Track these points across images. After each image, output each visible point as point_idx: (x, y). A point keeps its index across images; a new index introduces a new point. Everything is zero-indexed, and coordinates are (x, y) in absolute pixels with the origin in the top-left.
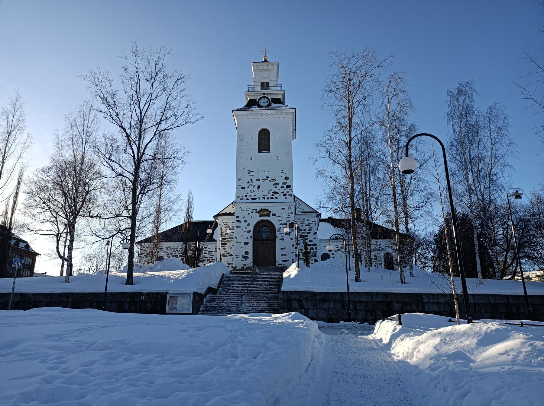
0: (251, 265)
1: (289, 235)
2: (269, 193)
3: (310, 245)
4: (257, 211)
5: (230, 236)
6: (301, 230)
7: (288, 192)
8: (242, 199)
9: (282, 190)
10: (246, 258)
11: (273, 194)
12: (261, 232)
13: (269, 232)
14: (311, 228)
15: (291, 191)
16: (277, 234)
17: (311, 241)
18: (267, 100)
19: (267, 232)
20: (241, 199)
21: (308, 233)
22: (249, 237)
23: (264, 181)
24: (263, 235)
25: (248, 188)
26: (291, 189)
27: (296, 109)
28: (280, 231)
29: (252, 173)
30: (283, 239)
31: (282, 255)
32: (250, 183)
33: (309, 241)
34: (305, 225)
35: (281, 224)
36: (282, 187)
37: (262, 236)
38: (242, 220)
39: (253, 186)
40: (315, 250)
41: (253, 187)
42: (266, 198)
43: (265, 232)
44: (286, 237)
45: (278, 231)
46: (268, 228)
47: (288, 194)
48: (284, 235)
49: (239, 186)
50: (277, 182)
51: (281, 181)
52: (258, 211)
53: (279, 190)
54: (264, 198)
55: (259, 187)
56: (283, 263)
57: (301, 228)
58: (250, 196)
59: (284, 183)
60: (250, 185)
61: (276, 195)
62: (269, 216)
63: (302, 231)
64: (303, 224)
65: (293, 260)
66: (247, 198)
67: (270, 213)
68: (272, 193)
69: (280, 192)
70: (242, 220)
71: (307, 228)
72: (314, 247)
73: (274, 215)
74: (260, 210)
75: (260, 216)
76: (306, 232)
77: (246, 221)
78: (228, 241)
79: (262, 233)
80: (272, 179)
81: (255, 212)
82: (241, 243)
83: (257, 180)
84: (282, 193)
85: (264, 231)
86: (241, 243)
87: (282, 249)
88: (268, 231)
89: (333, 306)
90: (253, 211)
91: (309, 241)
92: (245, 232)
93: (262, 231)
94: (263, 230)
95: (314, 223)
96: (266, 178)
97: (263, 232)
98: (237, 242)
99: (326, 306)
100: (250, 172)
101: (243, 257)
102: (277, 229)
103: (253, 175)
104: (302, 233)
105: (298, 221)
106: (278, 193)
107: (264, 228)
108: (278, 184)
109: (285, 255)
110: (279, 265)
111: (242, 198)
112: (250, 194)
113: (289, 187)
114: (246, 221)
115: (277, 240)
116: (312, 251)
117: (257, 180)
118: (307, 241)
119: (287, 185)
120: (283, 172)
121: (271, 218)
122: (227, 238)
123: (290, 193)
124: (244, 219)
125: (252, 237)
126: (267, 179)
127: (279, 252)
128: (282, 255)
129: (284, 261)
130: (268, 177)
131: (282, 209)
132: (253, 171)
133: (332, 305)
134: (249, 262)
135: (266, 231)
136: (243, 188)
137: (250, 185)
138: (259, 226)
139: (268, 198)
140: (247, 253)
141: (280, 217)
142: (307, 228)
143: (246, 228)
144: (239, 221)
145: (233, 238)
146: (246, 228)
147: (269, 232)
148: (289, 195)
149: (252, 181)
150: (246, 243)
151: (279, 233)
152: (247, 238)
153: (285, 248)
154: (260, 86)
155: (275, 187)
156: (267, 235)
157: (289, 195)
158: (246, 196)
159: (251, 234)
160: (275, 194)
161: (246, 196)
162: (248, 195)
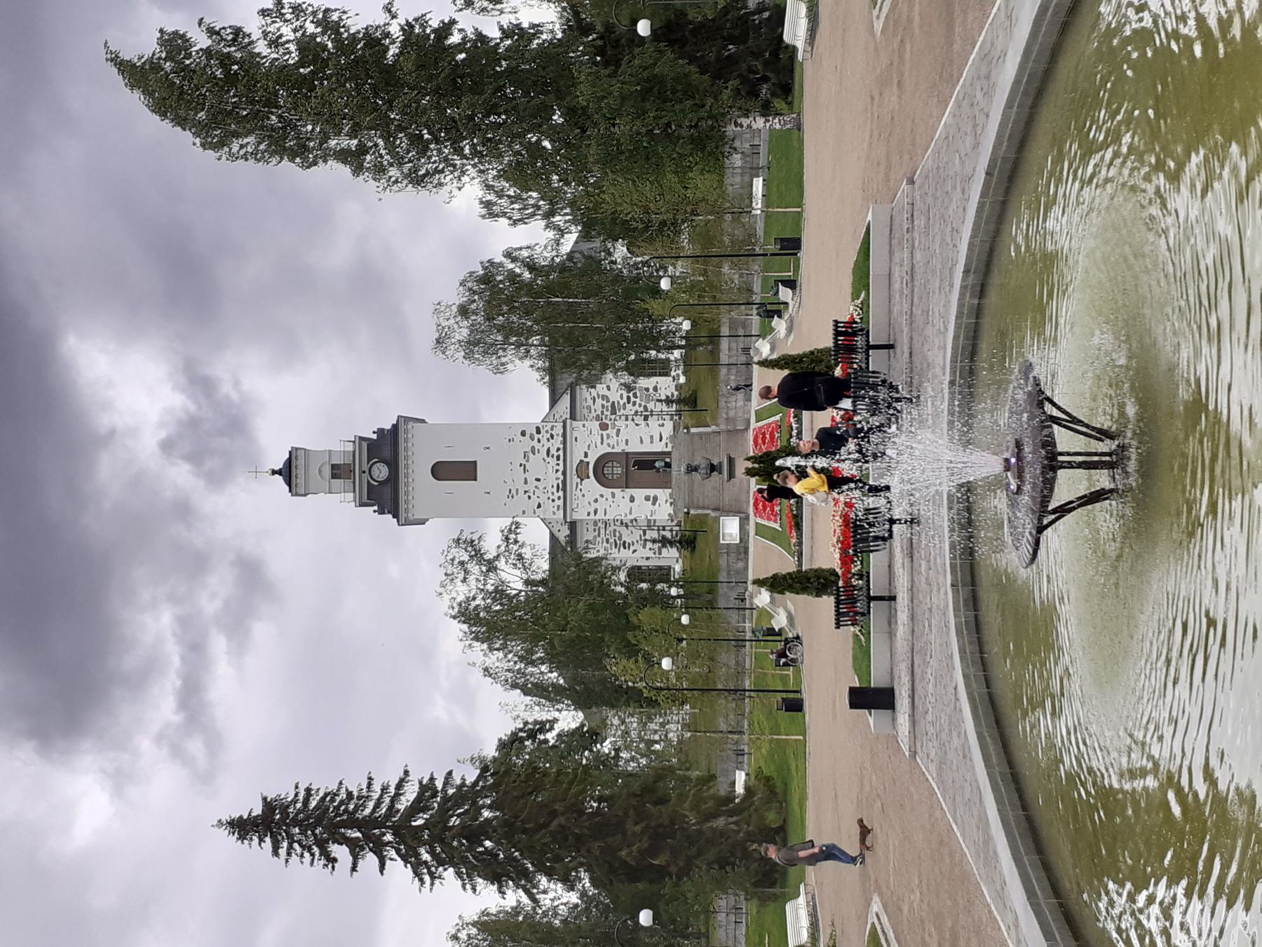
3: (628, 398)
6: (602, 413)
7: (547, 432)
8: (558, 507)
9: (544, 441)
10: (655, 499)
14: (598, 395)
17: (622, 395)
19: (613, 467)
29: (514, 492)
30: (627, 441)
31: (652, 442)
32: (531, 495)
35: (602, 443)
36: (539, 441)
38: (594, 506)
44: (623, 437)
45: (613, 448)
48: (620, 438)
51: (527, 443)
52: (579, 480)
54: (557, 471)
55: (538, 480)
56: (664, 440)
57: (599, 413)
58: (553, 493)
59: (532, 438)
61: (553, 451)
62: (588, 463)
64: (593, 408)
69: (549, 444)
70: (594, 506)
71: (599, 402)
73: (586, 455)
75: (588, 477)
77: (596, 501)
78: (620, 538)
83: (526, 482)
84: (548, 440)
87: (642, 441)
97: (613, 474)
100: (511, 495)
101: (654, 504)
102: (610, 450)
103: (517, 490)
108: (533, 447)
109: (652, 437)
113: (538, 431)
114: (596, 501)
115: (629, 449)
116: (638, 394)
117: (526, 482)
121: (592, 460)
123: (549, 428)
124: (592, 503)
127: (647, 448)
128: (652, 442)
129: (661, 440)
134: (663, 494)
136: (539, 506)
138: (602, 480)
140: (647, 498)
142: (599, 402)
144: (596, 512)
145: (615, 530)
148: (552, 430)
150: (632, 499)
157: (552, 430)
161: (553, 501)
162: (552, 497)
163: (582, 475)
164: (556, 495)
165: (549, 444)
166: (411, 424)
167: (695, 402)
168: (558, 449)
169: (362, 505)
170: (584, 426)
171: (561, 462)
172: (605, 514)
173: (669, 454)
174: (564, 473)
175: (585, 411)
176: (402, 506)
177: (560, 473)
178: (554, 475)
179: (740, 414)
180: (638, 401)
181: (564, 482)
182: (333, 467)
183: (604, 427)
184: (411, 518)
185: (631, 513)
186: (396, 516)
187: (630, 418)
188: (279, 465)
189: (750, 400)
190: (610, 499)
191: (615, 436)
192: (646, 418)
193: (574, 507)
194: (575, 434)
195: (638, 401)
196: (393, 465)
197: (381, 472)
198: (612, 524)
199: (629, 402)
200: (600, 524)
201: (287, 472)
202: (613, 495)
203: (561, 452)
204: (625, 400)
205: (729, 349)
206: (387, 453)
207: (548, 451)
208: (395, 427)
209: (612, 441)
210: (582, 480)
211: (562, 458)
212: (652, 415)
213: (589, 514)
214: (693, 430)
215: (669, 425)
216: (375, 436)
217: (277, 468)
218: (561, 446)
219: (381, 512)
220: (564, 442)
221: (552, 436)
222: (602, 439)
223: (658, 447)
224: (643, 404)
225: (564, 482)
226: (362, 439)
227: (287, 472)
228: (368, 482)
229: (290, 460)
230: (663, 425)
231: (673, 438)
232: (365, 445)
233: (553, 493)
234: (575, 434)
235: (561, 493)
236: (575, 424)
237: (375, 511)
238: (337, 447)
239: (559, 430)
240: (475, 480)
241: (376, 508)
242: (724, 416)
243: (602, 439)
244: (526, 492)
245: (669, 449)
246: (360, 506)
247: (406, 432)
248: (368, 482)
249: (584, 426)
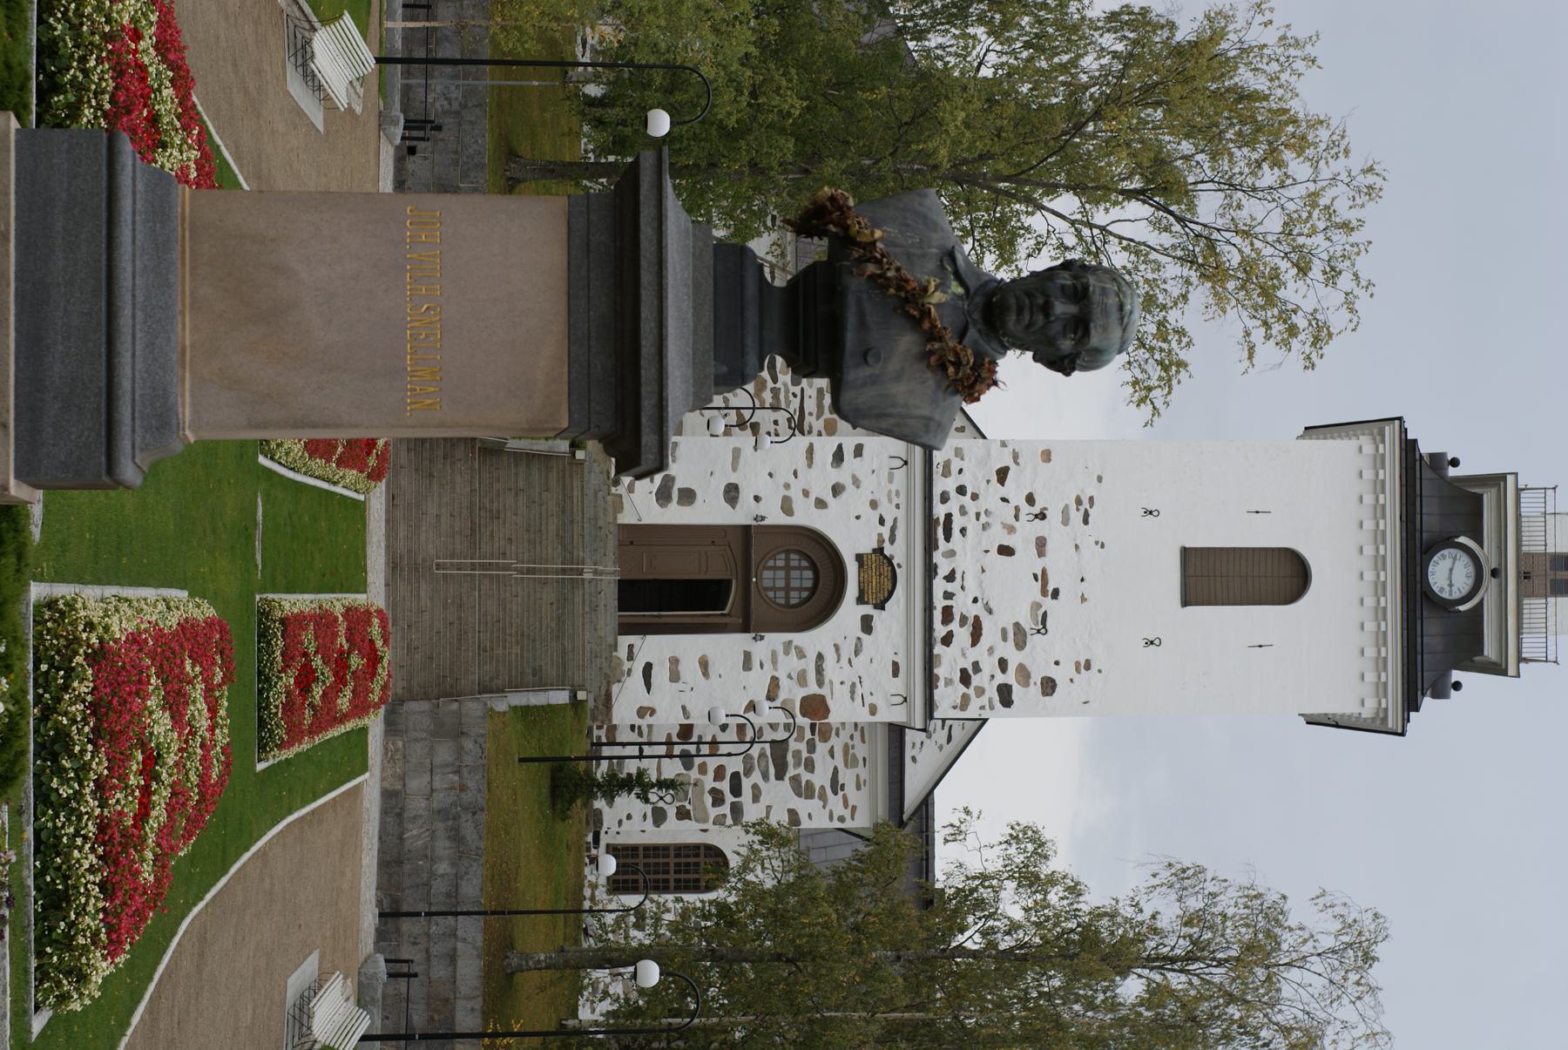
0: (626, 518)
1: (771, 697)
2: (975, 600)
3: (736, 790)
4: (887, 545)
5: (787, 391)
6: (811, 747)
7: (980, 692)
8: (946, 473)
9: (989, 665)
11: (971, 621)
12: (787, 560)
13: (787, 598)
14: (823, 797)
15: (982, 708)
16: (775, 640)
18: (1465, 590)
19: (787, 589)
20: (947, 465)
21: (795, 780)
22: (761, 509)
23: (1035, 577)
24: (775, 568)
25: (1004, 500)
26: (992, 708)
27: (1402, 734)
28: (787, 652)
29: (1078, 518)
31: (674, 662)
32: (1025, 508)
33: (755, 787)
34: (836, 769)
35: (820, 657)
36: (1003, 664)
37: (771, 563)
38: (843, 475)
39: (1011, 521)
40: (713, 812)
41: (1005, 526)
42: (950, 587)
43: (788, 578)
45: (788, 645)
46: (805, 594)
47: (971, 691)
48: (769, 672)
49: (1015, 457)
50: (1034, 641)
51: (1039, 656)
53: (991, 650)
54: (950, 577)
55: (1005, 551)
57: (822, 748)
58: (963, 511)
59: (1024, 674)
60: (1017, 509)
61: (962, 635)
62: (861, 600)
63: (805, 755)
64: (839, 760)
65: (653, 712)
66: (953, 494)
67: (876, 607)
68: (977, 618)
69: (975, 654)
70: (843, 475)
71: (821, 778)
72: (725, 809)
73: (867, 624)
74: (889, 560)
75: (859, 558)
76: (801, 770)
77: (837, 490)
79: (780, 563)
80: (1045, 614)
81: (880, 535)
82: (734, 469)
83: (1041, 545)
84: (976, 667)
85: (795, 574)
86: (734, 469)
87: (704, 665)
88: (794, 594)
89: (441, 871)
90: (889, 523)
91: (755, 787)
92: (787, 486)
93: (794, 563)
94: (800, 568)
95: (847, 813)
96: (1050, 588)
97: (788, 568)
98: (736, 453)
99: (443, 846)
100: (1085, 509)
102: (798, 638)
103: (1066, 521)
104: (797, 753)
105: (857, 735)
106: (974, 644)
107: (809, 574)
108: (1020, 644)
109: (675, 677)
110: (631, 647)
111: (954, 469)
112: (972, 507)
114: (837, 490)
116: (708, 800)
117: (1041, 545)
118: (756, 777)
119: (1016, 689)
120: (1078, 670)
121: (849, 611)
122: (775, 380)
123: (975, 703)
124: (847, 481)
125: (762, 523)
126: (1044, 592)
127: (689, 646)
128: (674, 662)
129: (648, 670)
130: (1056, 594)
131: (896, 666)
132: (1086, 521)
133: (443, 868)
135: (795, 584)
136: (1002, 474)
137: (1017, 509)
139: (948, 595)
140: (688, 496)
141: (857, 653)
142: (821, 778)
143: (806, 493)
144: (838, 457)
146: (806, 493)
147: (787, 598)
149: (1036, 516)
151: (780, 649)
152: (757, 499)
153: (706, 673)
154: (1550, 550)
155: (1004, 631)
156: (774, 589)
158: (961, 490)
159: (776, 517)
160: (968, 629)
162: (967, 500)
163: (879, 567)
164: (953, 507)
165: (975, 654)
166: (1368, 711)
167: (555, 789)
168: (947, 640)
169: (1498, 480)
170: (873, 710)
171: (939, 603)
172: (810, 451)
173: (626, 629)
174: (930, 570)
175: (861, 751)
176: (1391, 474)
177: (943, 571)
178: (960, 564)
179: (418, 750)
180: (709, 782)
181: (930, 546)
183: (815, 707)
184: (1366, 442)
185: (736, 453)
186: (1409, 447)
187: (732, 735)
189: (388, 795)
190: (795, 494)
191: (784, 682)
192: (686, 731)
193: (900, 475)
194: (898, 685)
195: (709, 782)
198: (783, 424)
199: (736, 777)
200: (818, 425)
202: (787, 506)
203: (940, 630)
204: (746, 784)
205: (452, 958)
206: (1433, 631)
207: (976, 636)
209: (789, 664)
210: (879, 551)
211: (938, 615)
212: (669, 743)
213: (858, 451)
214: (561, 697)
215: (623, 712)
216: (1456, 675)
218: (938, 649)
219: (1438, 461)
220: (930, 661)
221: (965, 679)
222: (819, 671)
223: (655, 648)
224: (694, 774)
225: (930, 546)
226: (1498, 669)
228: (1480, 543)
230: (642, 712)
231: (611, 675)
232: (1490, 651)
233: (963, 511)
234: (898, 685)
235: (940, 511)
236: (898, 716)
237: (1455, 463)
239: (946, 698)
240: (1185, 552)
241: (1452, 472)
242: (468, 744)
243: (819, 671)
244: (1042, 516)
245: (625, 641)
246: (1502, 478)
247: (1381, 689)
248: (1480, 543)
249: (873, 710)
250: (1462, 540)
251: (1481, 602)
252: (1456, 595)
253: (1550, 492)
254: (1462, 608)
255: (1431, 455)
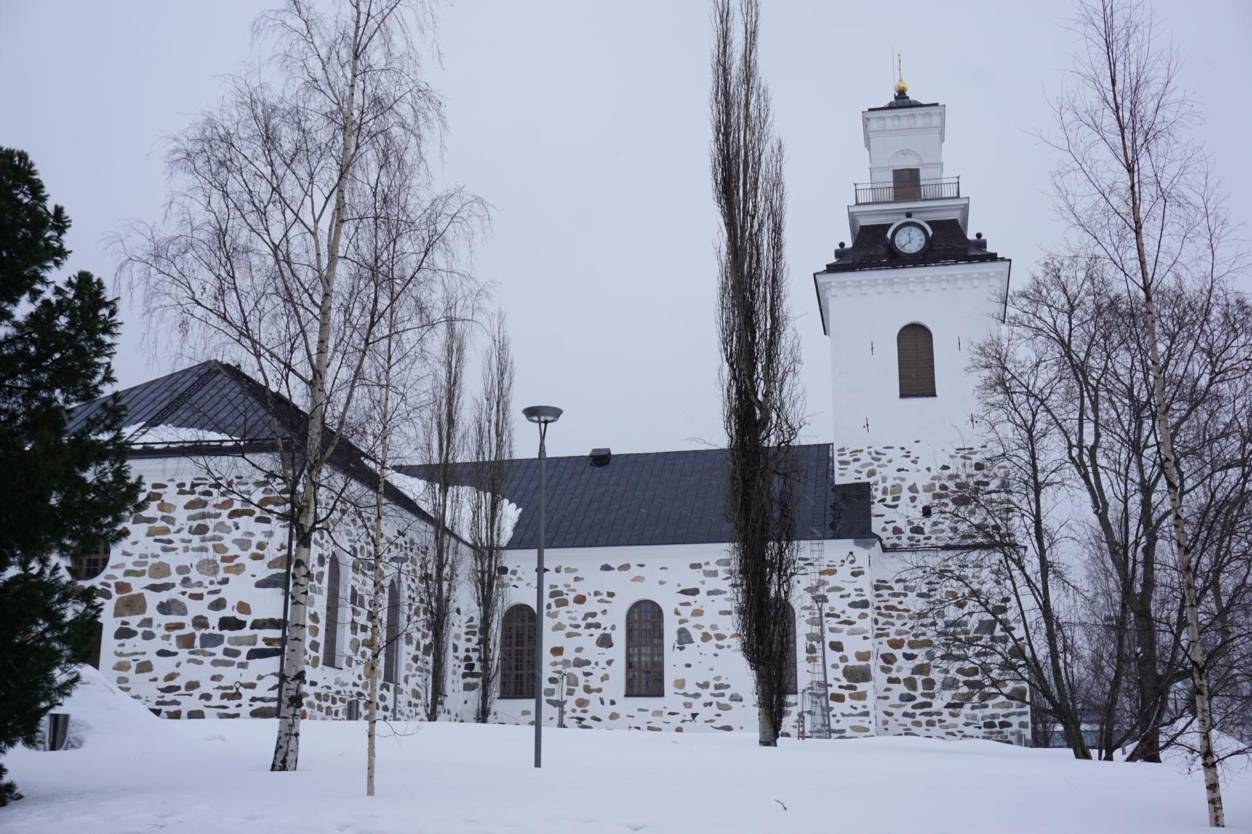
18: (919, 232)
27: (1010, 260)
169: (853, 218)
182: (914, 173)
188: (912, 95)
196: (924, 258)
197: (911, 241)
201: (902, 101)
208: (993, 257)
217: (908, 94)
226: (965, 209)
227: (902, 101)
228: (890, 225)
229: (918, 105)
237: (842, 245)
238: (948, 174)
250: (889, 235)
251: (929, 223)
252: (923, 237)
253: (858, 187)
254: (930, 233)
255: (837, 256)
